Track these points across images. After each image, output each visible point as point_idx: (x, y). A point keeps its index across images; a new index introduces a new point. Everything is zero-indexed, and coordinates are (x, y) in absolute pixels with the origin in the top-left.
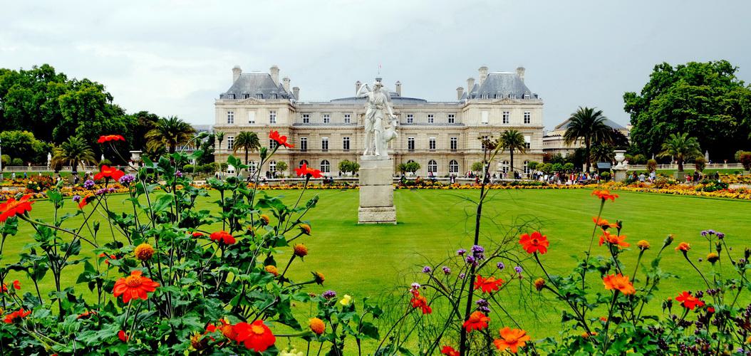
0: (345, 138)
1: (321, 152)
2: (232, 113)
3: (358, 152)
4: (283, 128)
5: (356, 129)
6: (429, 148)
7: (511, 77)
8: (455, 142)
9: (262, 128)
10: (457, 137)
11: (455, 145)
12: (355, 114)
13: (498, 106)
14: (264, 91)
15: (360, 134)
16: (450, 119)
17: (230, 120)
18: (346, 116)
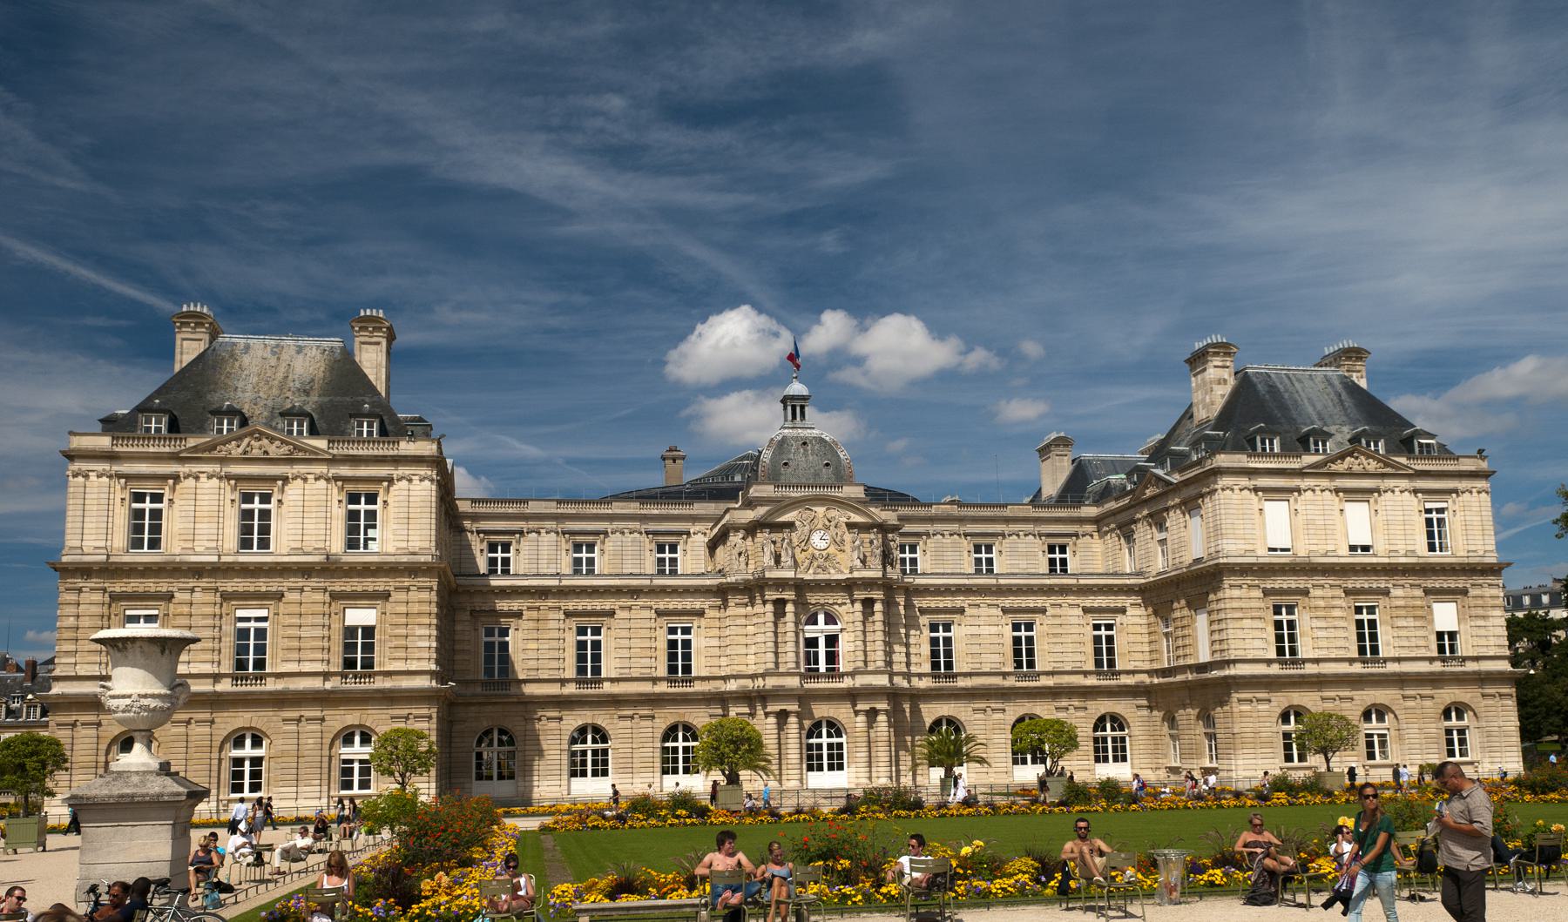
0: (673, 631)
1: (571, 689)
2: (157, 498)
3: (732, 686)
4: (413, 570)
5: (723, 593)
6: (1010, 668)
7: (1328, 380)
8: (1110, 639)
9: (306, 570)
10: (1119, 618)
11: (1111, 651)
12: (699, 541)
13: (1325, 483)
14: (321, 408)
15: (742, 611)
16: (1052, 562)
17: (145, 528)
18: (661, 549)
